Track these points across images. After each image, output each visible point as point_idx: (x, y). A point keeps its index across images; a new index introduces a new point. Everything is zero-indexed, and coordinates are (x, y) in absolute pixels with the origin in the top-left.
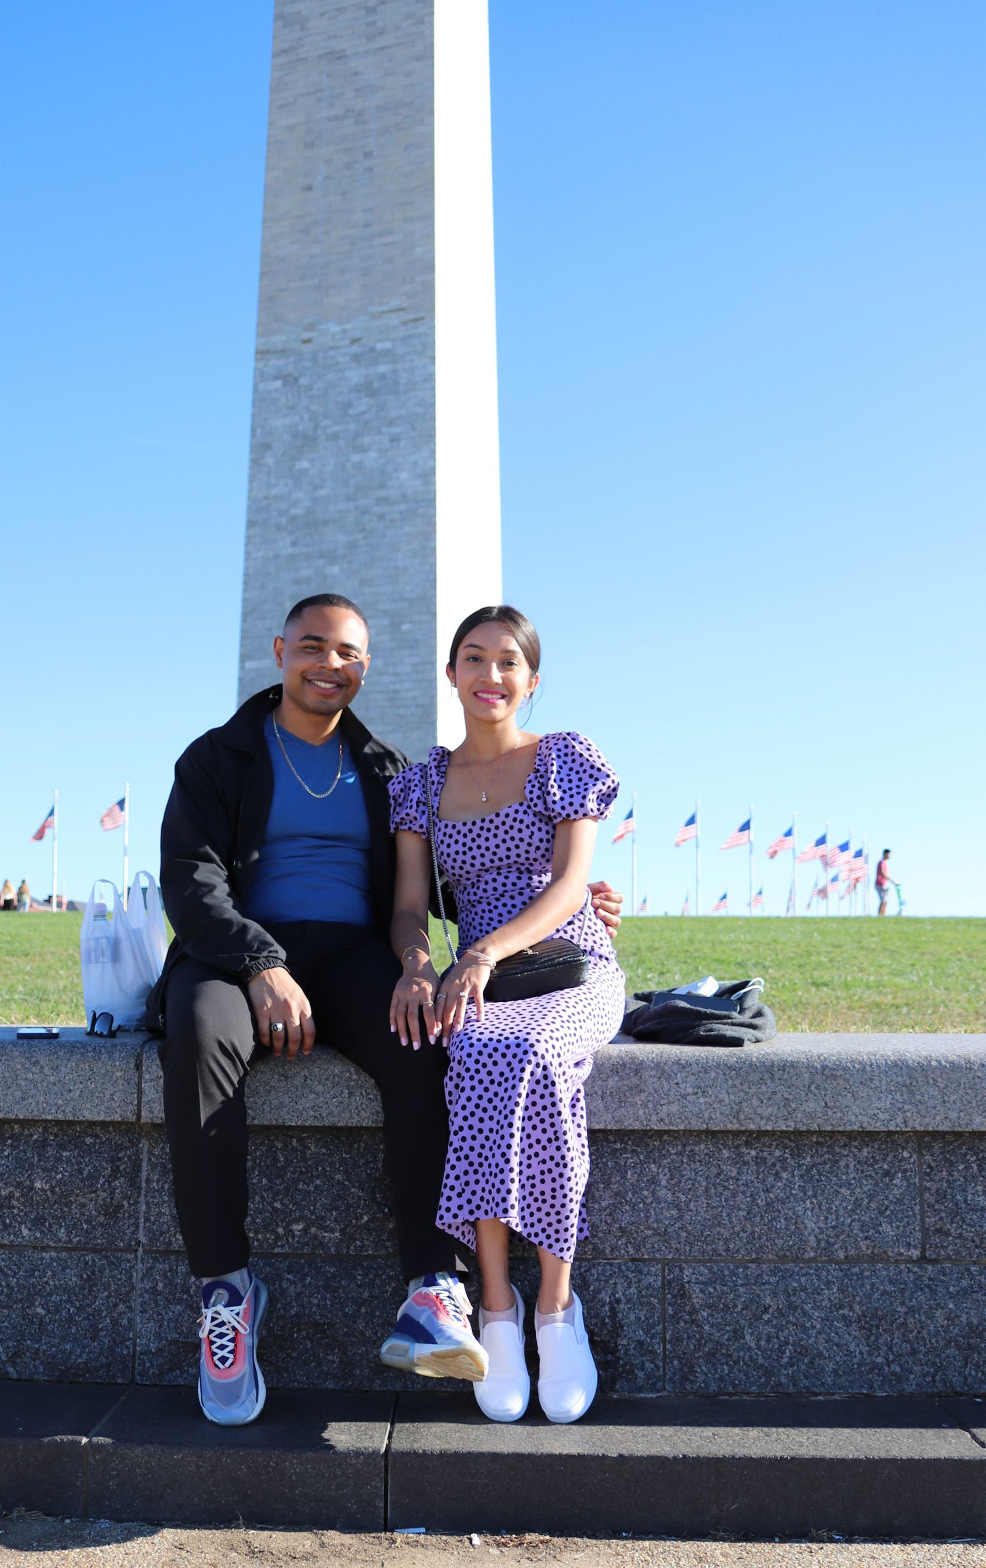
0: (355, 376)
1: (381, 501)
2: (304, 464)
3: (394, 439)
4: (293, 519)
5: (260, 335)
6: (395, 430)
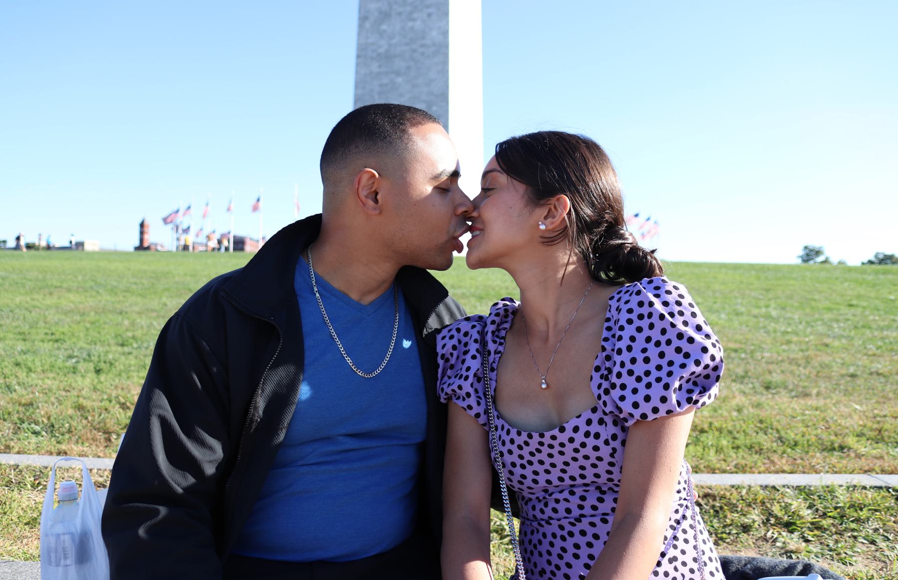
1: (422, 46)
4: (379, 55)
6: (430, 10)
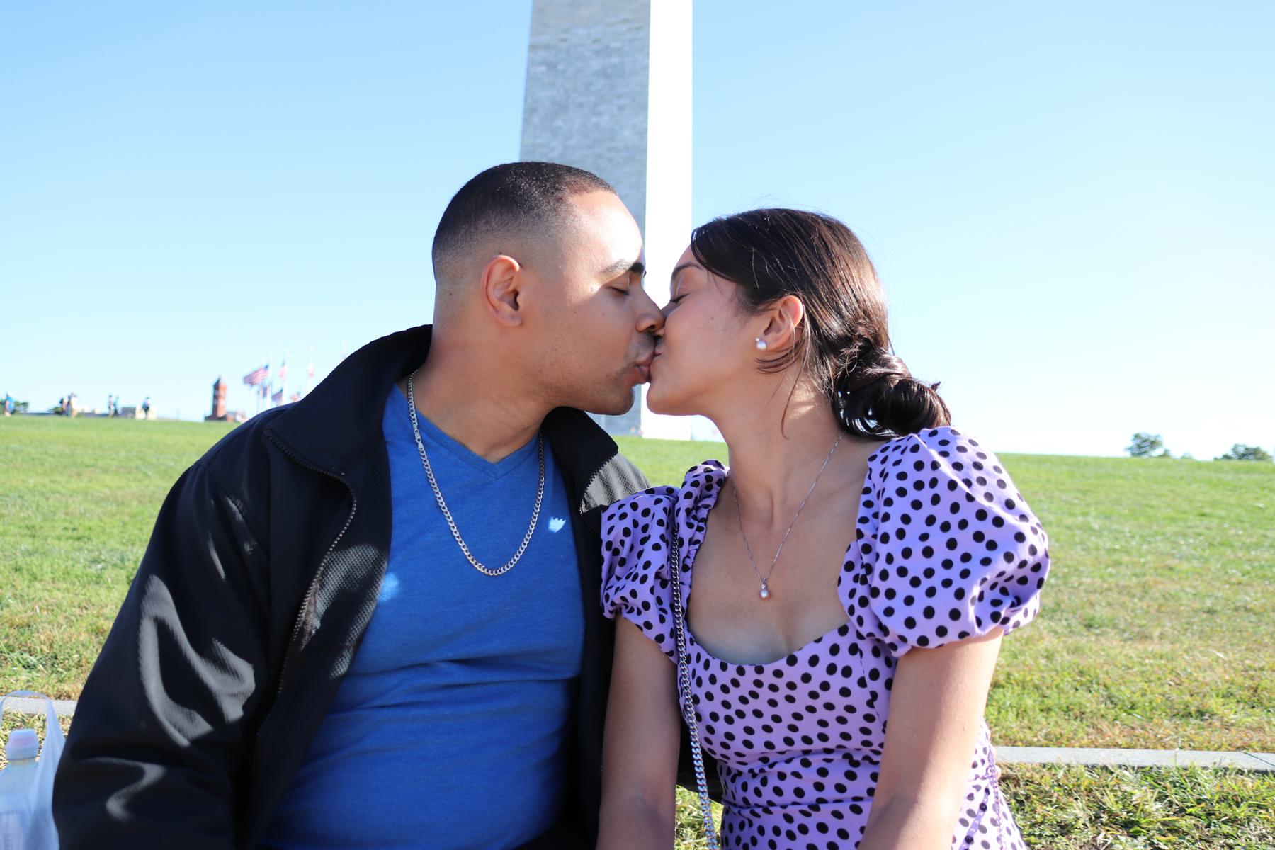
0: (596, 64)
1: (610, 149)
2: (559, 123)
3: (621, 108)
5: (532, 34)
6: (623, 102)
